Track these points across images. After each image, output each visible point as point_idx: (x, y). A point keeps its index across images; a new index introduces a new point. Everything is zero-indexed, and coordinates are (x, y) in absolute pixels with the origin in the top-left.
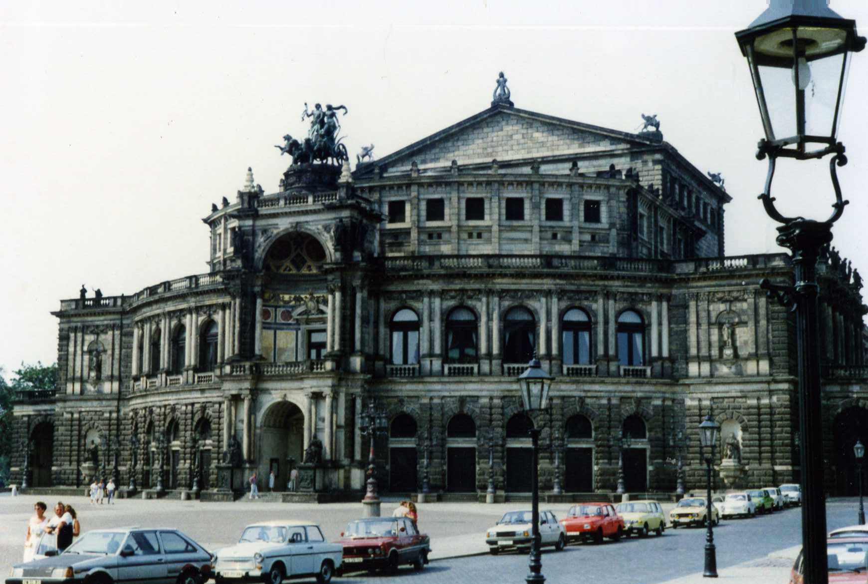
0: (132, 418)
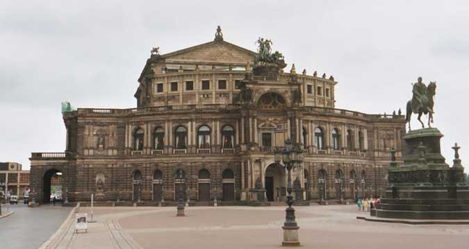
0: (130, 168)
